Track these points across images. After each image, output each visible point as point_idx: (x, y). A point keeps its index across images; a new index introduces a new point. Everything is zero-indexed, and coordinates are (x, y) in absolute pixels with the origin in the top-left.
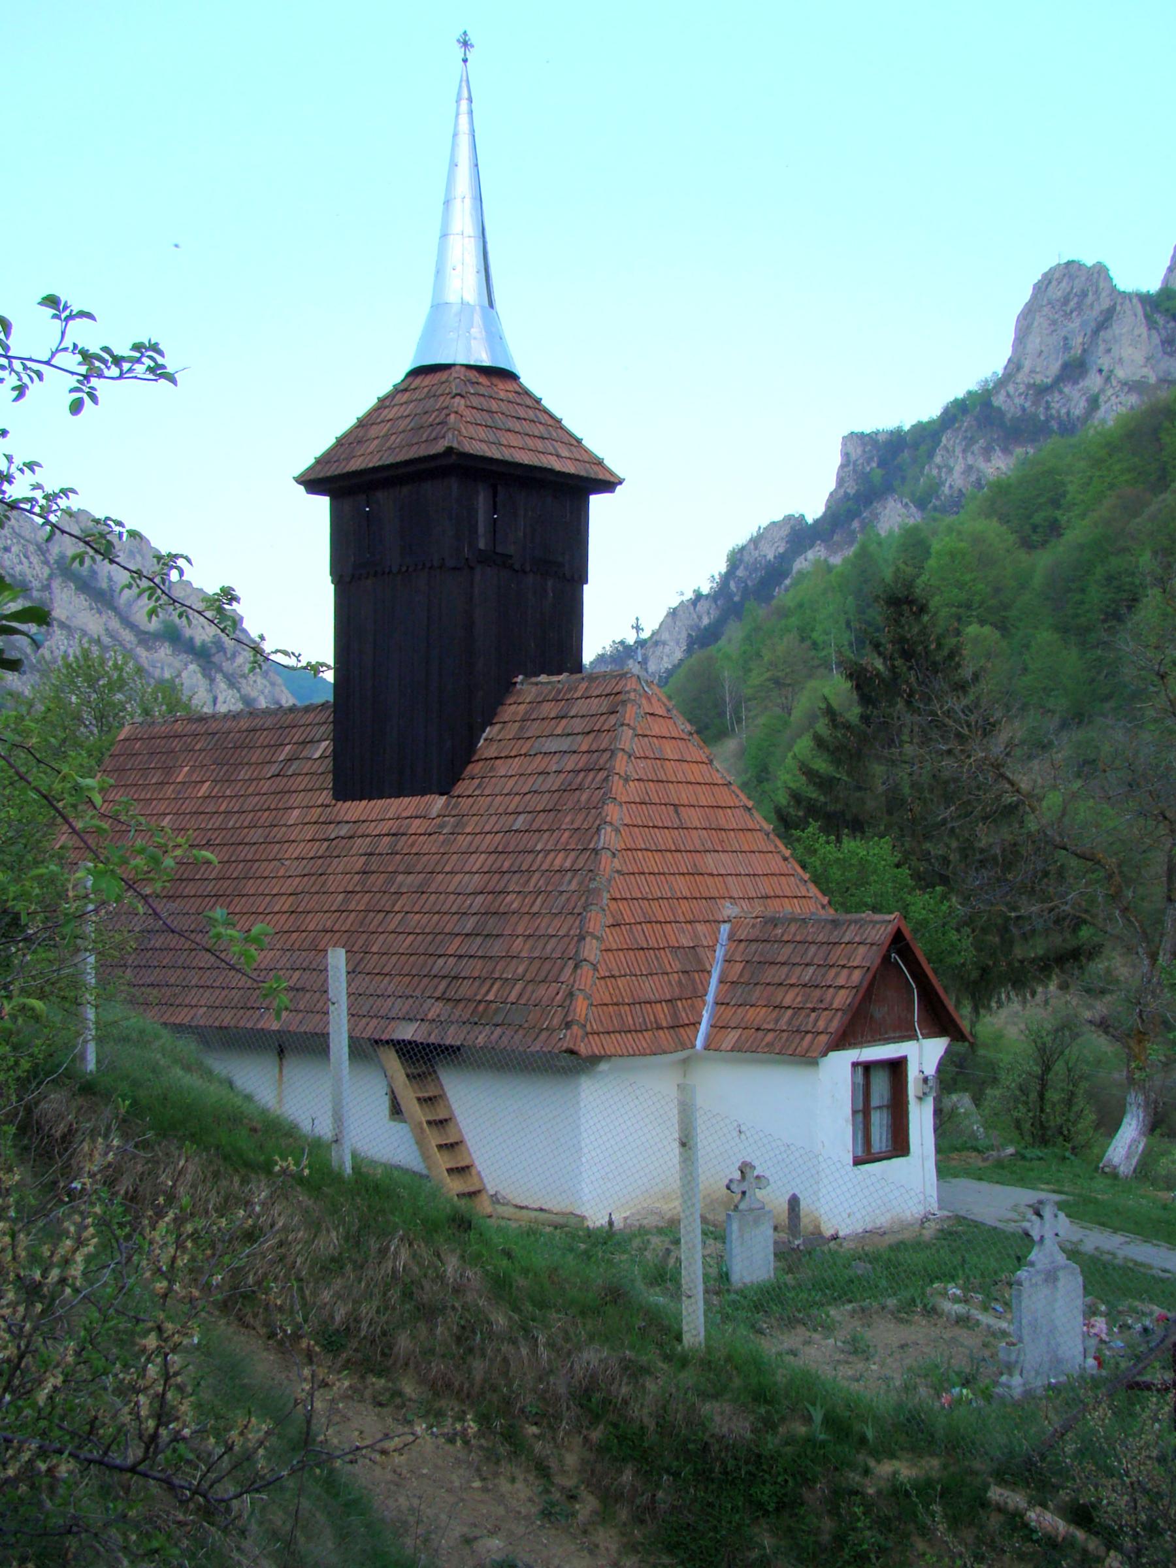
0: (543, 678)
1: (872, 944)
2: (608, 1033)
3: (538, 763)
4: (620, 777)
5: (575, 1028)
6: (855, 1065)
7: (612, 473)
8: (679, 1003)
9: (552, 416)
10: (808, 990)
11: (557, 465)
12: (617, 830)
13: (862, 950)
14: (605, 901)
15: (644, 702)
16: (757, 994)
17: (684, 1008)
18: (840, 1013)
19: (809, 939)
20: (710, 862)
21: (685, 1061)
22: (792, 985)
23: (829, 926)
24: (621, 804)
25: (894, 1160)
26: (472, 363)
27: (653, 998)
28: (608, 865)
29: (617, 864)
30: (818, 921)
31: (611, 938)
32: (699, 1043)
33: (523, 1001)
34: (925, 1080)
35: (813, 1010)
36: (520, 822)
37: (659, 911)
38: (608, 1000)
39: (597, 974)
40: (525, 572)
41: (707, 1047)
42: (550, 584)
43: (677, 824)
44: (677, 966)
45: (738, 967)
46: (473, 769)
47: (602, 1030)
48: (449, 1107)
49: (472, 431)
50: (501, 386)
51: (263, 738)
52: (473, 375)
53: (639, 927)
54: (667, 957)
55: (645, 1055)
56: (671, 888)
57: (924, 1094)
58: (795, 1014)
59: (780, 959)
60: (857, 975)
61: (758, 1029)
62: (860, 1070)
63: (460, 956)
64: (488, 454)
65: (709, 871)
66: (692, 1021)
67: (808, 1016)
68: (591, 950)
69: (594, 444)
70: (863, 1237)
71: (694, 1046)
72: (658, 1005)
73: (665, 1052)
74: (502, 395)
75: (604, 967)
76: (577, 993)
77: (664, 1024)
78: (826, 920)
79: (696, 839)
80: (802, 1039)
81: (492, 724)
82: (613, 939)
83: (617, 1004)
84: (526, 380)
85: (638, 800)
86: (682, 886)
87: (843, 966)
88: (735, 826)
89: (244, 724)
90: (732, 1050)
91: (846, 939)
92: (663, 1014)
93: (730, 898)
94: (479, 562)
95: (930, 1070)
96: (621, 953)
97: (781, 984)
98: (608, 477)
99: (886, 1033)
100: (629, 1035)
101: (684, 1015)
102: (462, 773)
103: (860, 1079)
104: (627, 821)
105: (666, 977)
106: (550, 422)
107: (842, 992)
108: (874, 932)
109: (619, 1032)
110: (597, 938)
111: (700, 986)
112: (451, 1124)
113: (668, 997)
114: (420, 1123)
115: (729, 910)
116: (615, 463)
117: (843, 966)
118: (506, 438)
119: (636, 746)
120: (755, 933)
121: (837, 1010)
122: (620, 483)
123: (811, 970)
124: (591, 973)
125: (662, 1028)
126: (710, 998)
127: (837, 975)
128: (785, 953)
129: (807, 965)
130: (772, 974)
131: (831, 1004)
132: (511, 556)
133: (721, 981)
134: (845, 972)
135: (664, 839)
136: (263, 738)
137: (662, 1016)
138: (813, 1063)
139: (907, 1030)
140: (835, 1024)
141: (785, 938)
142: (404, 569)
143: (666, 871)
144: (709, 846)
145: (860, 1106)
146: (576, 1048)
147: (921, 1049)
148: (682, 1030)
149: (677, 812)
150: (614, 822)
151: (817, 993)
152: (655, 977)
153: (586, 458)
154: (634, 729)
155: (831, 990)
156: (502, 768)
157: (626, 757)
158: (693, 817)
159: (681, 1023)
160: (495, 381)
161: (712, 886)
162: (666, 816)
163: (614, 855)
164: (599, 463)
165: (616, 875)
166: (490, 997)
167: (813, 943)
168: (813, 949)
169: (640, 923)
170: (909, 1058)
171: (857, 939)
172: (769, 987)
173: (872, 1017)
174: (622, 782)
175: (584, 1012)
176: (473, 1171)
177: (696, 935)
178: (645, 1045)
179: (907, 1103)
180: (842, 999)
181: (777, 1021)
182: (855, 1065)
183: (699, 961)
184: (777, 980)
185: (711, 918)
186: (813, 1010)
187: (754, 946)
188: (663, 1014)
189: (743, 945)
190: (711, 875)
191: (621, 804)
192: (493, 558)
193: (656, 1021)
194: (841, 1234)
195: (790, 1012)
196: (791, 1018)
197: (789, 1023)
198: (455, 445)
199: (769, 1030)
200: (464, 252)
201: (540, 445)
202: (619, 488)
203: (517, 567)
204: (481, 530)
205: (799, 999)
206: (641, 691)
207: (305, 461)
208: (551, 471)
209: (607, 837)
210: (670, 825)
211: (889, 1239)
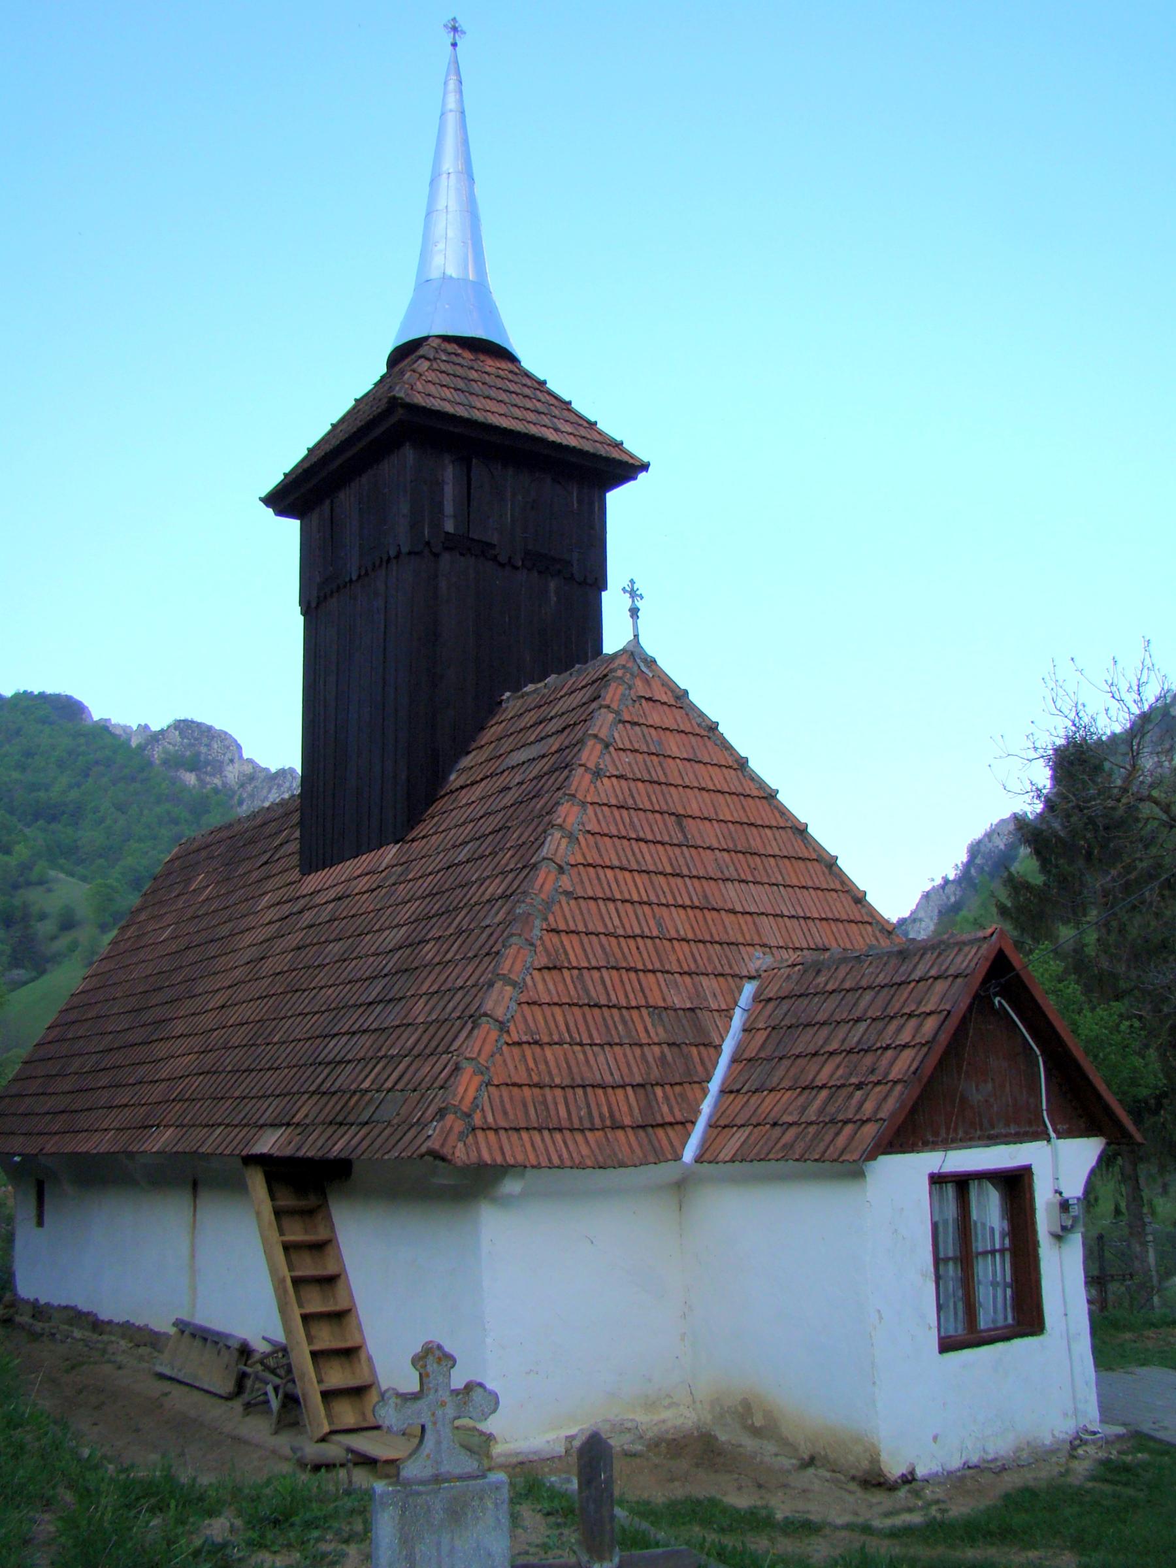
0: (530, 688)
1: (956, 977)
2: (517, 1130)
3: (500, 782)
4: (587, 769)
5: (450, 1118)
6: (937, 1180)
7: (632, 456)
8: (659, 1091)
9: (556, 398)
10: (854, 1058)
11: (552, 436)
12: (571, 837)
13: (940, 986)
15: (639, 683)
16: (780, 1073)
17: (666, 1098)
18: (899, 1087)
19: (864, 983)
20: (732, 895)
21: (681, 1186)
22: (831, 1054)
23: (894, 961)
24: (583, 804)
25: (1017, 1342)
26: (450, 333)
27: (608, 1079)
28: (545, 881)
29: (565, 882)
30: (879, 957)
31: (540, 986)
32: (689, 1154)
33: (399, 1087)
34: (1065, 1206)
35: (859, 1086)
36: (464, 853)
37: (632, 954)
38: (522, 1078)
39: (506, 1038)
40: (516, 568)
41: (699, 1159)
42: (552, 585)
43: (678, 838)
44: (661, 1035)
45: (761, 1037)
46: (438, 806)
47: (503, 1124)
48: (339, 1258)
49: (432, 389)
50: (490, 362)
51: (268, 830)
52: (453, 347)
53: (596, 974)
54: (645, 1027)
55: (581, 1166)
56: (659, 925)
57: (1064, 1228)
58: (830, 1097)
59: (821, 1017)
60: (930, 1024)
61: (775, 1124)
62: (950, 1191)
63: (354, 1033)
64: (448, 408)
65: (729, 906)
66: (679, 1117)
67: (851, 1096)
68: (499, 1001)
69: (611, 426)
70: (962, 1479)
71: (678, 1158)
72: (620, 1092)
73: (622, 1165)
74: (488, 369)
75: (522, 1027)
76: (465, 1064)
77: (627, 1121)
78: (889, 954)
79: (708, 863)
80: (837, 1134)
81: (468, 753)
82: (545, 987)
83: (536, 1085)
84: (527, 363)
85: (613, 802)
86: (679, 922)
87: (910, 1015)
88: (777, 852)
89: (259, 821)
90: (732, 1161)
91: (916, 975)
92: (627, 1105)
93: (764, 945)
94: (447, 549)
95: (1074, 1189)
96: (557, 1010)
97: (815, 1054)
98: (625, 458)
99: (993, 1127)
100: (558, 1136)
101: (665, 1109)
102: (422, 813)
103: (951, 1210)
104: (592, 826)
105: (638, 1051)
106: (553, 401)
107: (908, 1054)
108: (959, 959)
109: (539, 1130)
110: (514, 984)
111: (699, 1068)
112: (341, 1284)
113: (638, 1079)
114: (283, 1280)
115: (759, 960)
116: (637, 447)
117: (910, 1015)
118: (478, 402)
119: (621, 736)
120: (787, 987)
121: (895, 1082)
122: (645, 467)
123: (862, 1026)
124: (494, 1034)
125: (623, 1128)
126: (714, 1086)
127: (900, 1029)
128: (825, 1009)
129: (858, 1020)
130: (806, 1041)
131: (887, 1074)
132: (493, 546)
133: (734, 1060)
134: (913, 1022)
135: (649, 856)
136: (268, 830)
137: (624, 1108)
138: (858, 1174)
139: (1030, 1123)
140: (890, 1105)
141: (829, 987)
142: (363, 572)
143: (654, 899)
144: (731, 872)
145: (950, 1248)
146: (446, 1151)
147: (1055, 1155)
148: (660, 1132)
149: (680, 824)
150: (568, 826)
151: (869, 1059)
152: (617, 1049)
153: (597, 437)
154: (617, 713)
155: (890, 1053)
156: (465, 797)
157: (599, 747)
158: (710, 834)
159: (659, 1120)
160: (482, 357)
161: (732, 928)
162: (665, 828)
163: (561, 870)
164: (618, 445)
165: (563, 899)
166: (365, 1085)
167: (869, 987)
168: (868, 996)
169: (598, 969)
170: (1035, 1169)
171: (933, 972)
172: (799, 1061)
173: (964, 1100)
174: (588, 777)
175: (471, 1093)
176: (363, 1356)
177: (698, 993)
178: (585, 1151)
179: (1036, 1244)
180: (904, 1063)
181: (804, 1109)
182: (937, 1180)
183: (699, 1028)
184: (811, 1049)
185: (727, 970)
186: (859, 1086)
187: (785, 1005)
188: (627, 1105)
189: (772, 1005)
190: (733, 911)
191: (583, 804)
192: (460, 544)
193: (612, 1115)
194: (921, 1472)
195: (824, 1093)
196: (826, 1103)
197: (821, 1111)
198: (402, 395)
199: (791, 1125)
200: (449, 226)
201: (531, 416)
202: (642, 476)
203: (503, 559)
204: (449, 508)
205: (840, 1072)
206: (635, 669)
207: (273, 479)
208: (542, 441)
209: (555, 845)
210: (666, 839)
211: (1012, 1481)
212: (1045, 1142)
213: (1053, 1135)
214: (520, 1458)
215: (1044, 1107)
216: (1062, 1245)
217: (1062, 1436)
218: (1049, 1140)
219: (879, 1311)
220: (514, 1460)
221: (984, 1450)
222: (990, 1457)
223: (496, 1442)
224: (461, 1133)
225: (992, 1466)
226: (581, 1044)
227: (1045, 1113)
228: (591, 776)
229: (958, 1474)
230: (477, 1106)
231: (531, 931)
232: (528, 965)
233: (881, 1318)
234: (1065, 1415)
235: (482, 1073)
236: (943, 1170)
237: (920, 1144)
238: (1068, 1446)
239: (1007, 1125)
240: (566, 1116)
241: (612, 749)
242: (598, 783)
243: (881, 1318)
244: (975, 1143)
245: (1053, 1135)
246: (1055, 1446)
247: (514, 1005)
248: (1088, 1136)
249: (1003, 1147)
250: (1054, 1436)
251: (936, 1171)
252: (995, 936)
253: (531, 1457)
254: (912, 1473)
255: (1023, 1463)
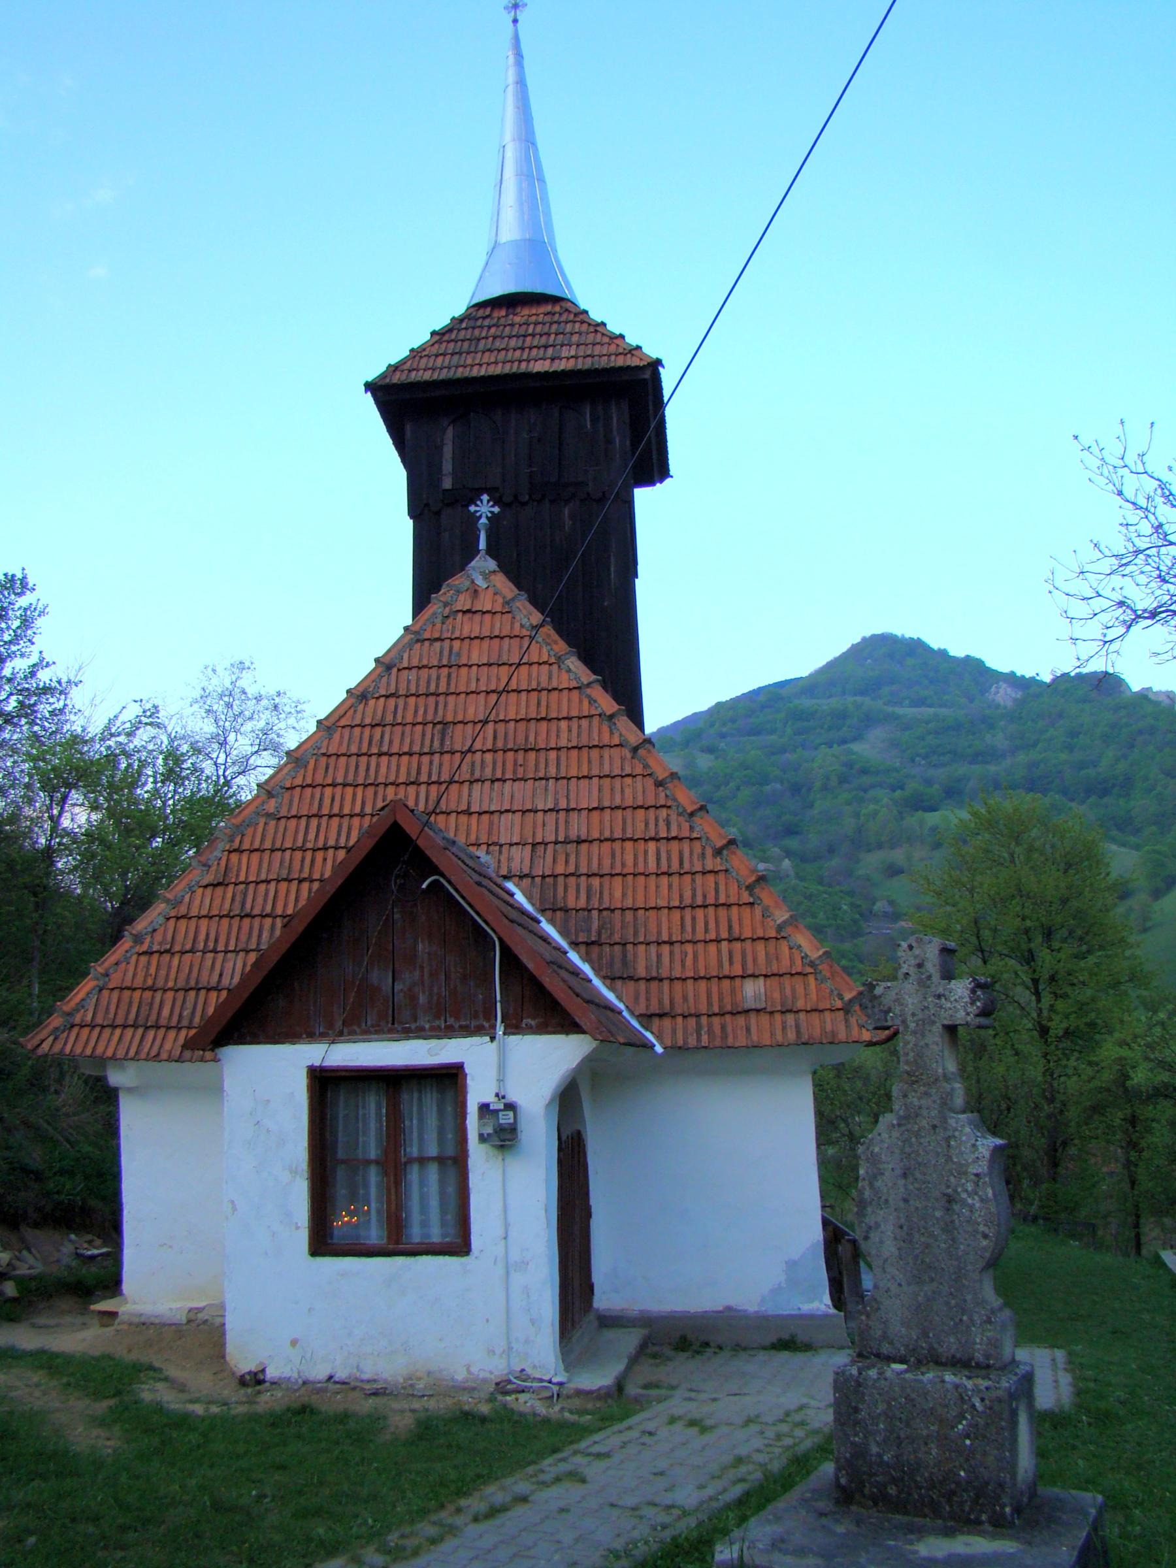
14: (217, 853)
55: (157, 1057)
139: (476, 1016)
170: (468, 1069)
194: (272, 1373)
212: (488, 1039)
213: (500, 1031)
214: (143, 1319)
215: (498, 998)
216: (509, 1159)
217: (482, 1375)
218: (493, 1039)
219: (233, 1202)
220: (136, 1320)
221: (358, 1367)
222: (365, 1376)
223: (127, 1303)
224: (57, 1029)
225: (367, 1386)
226: (215, 951)
227: (498, 1005)
228: (354, 701)
229: (319, 1385)
230: (83, 1007)
231: (211, 852)
232: (193, 883)
233: (235, 1209)
234: (492, 1352)
235: (98, 979)
236: (327, 1063)
237: (304, 1036)
238: (492, 1388)
239: (437, 1017)
240: (167, 1016)
241: (395, 670)
242: (361, 707)
243: (235, 1209)
244: (373, 1036)
245: (500, 1031)
246: (470, 1384)
247: (161, 920)
248: (567, 1033)
249: (421, 1042)
250: (468, 1370)
251: (317, 1063)
252: (386, 809)
253: (153, 1320)
254: (263, 1371)
255: (415, 1393)
